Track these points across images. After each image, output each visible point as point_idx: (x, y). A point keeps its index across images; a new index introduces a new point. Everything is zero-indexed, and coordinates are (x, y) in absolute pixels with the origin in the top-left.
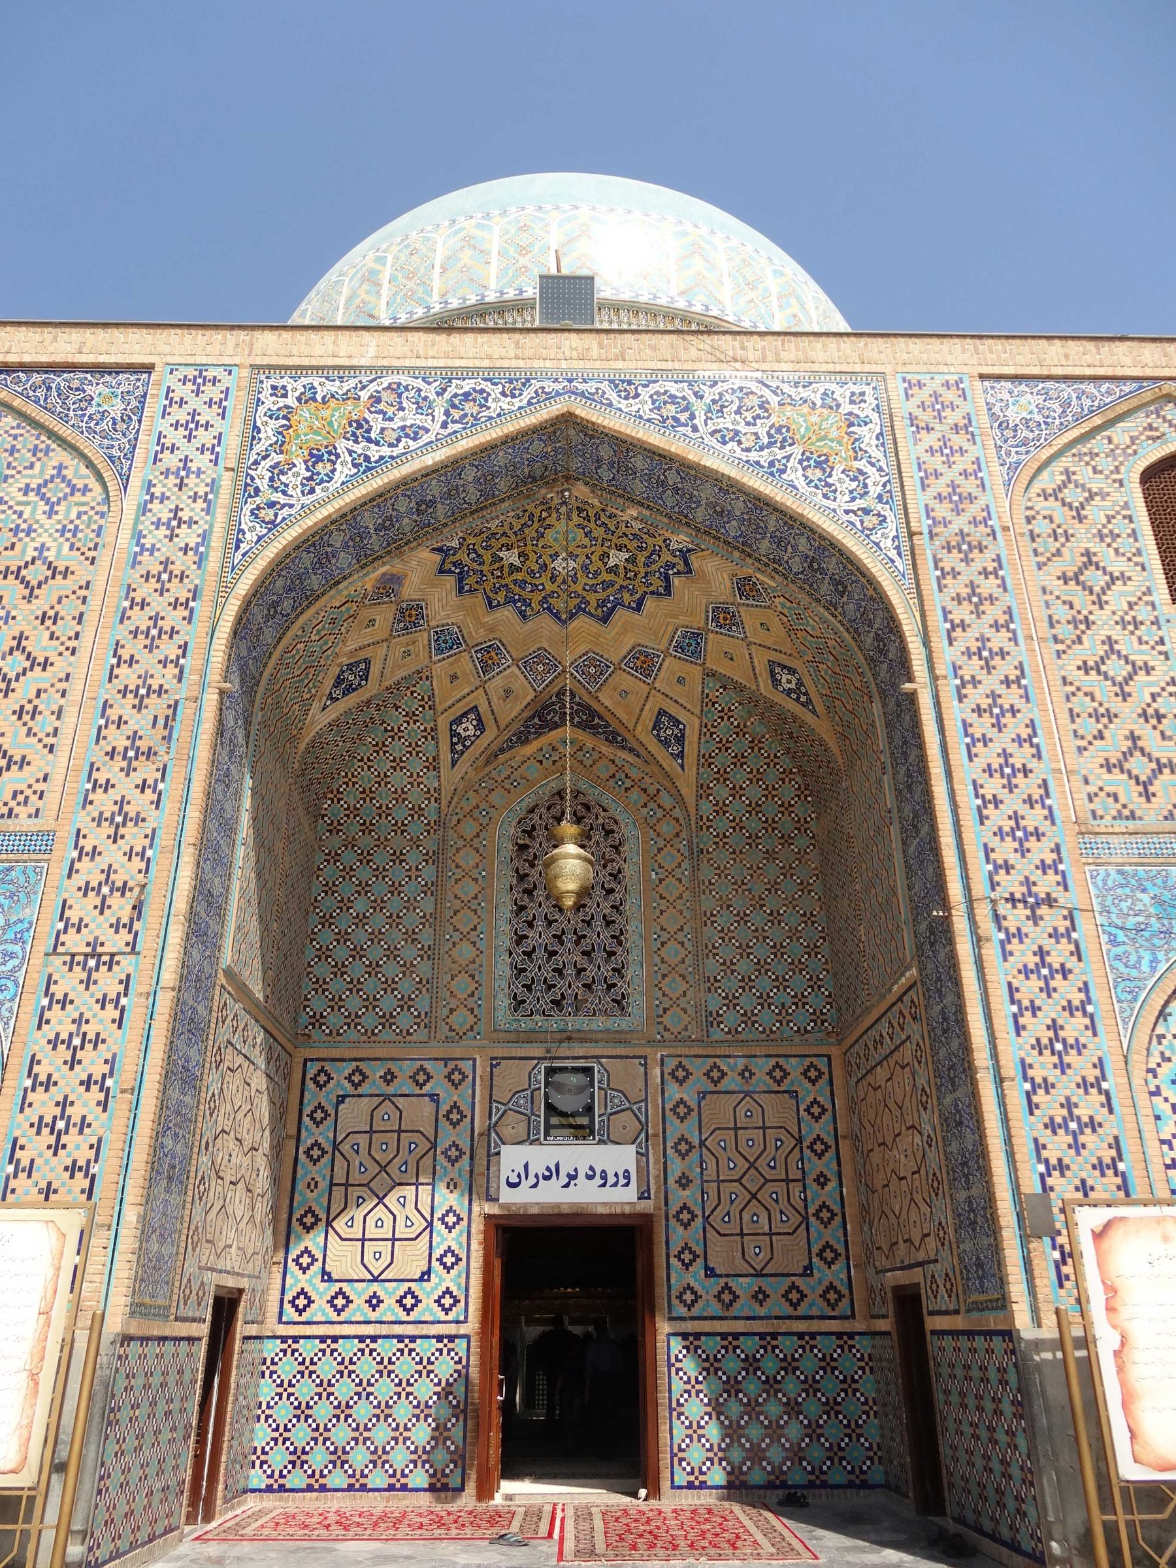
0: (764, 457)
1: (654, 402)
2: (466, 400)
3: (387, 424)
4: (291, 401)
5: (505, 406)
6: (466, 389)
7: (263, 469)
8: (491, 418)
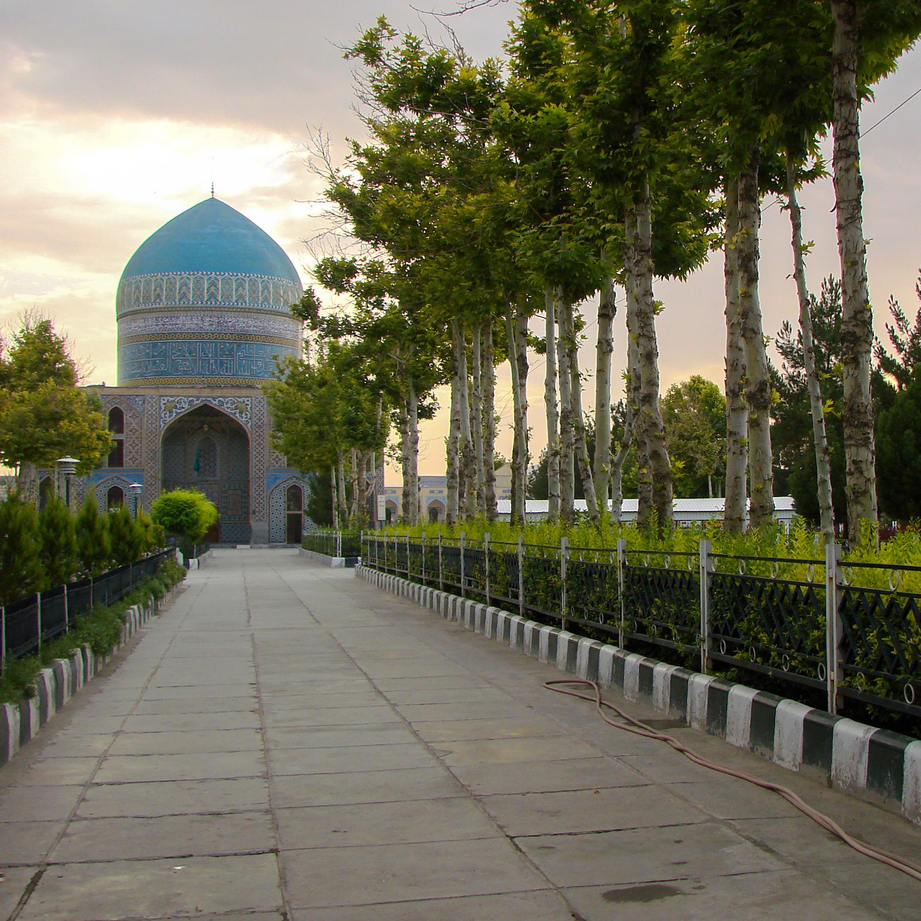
0: (233, 412)
7: (163, 415)
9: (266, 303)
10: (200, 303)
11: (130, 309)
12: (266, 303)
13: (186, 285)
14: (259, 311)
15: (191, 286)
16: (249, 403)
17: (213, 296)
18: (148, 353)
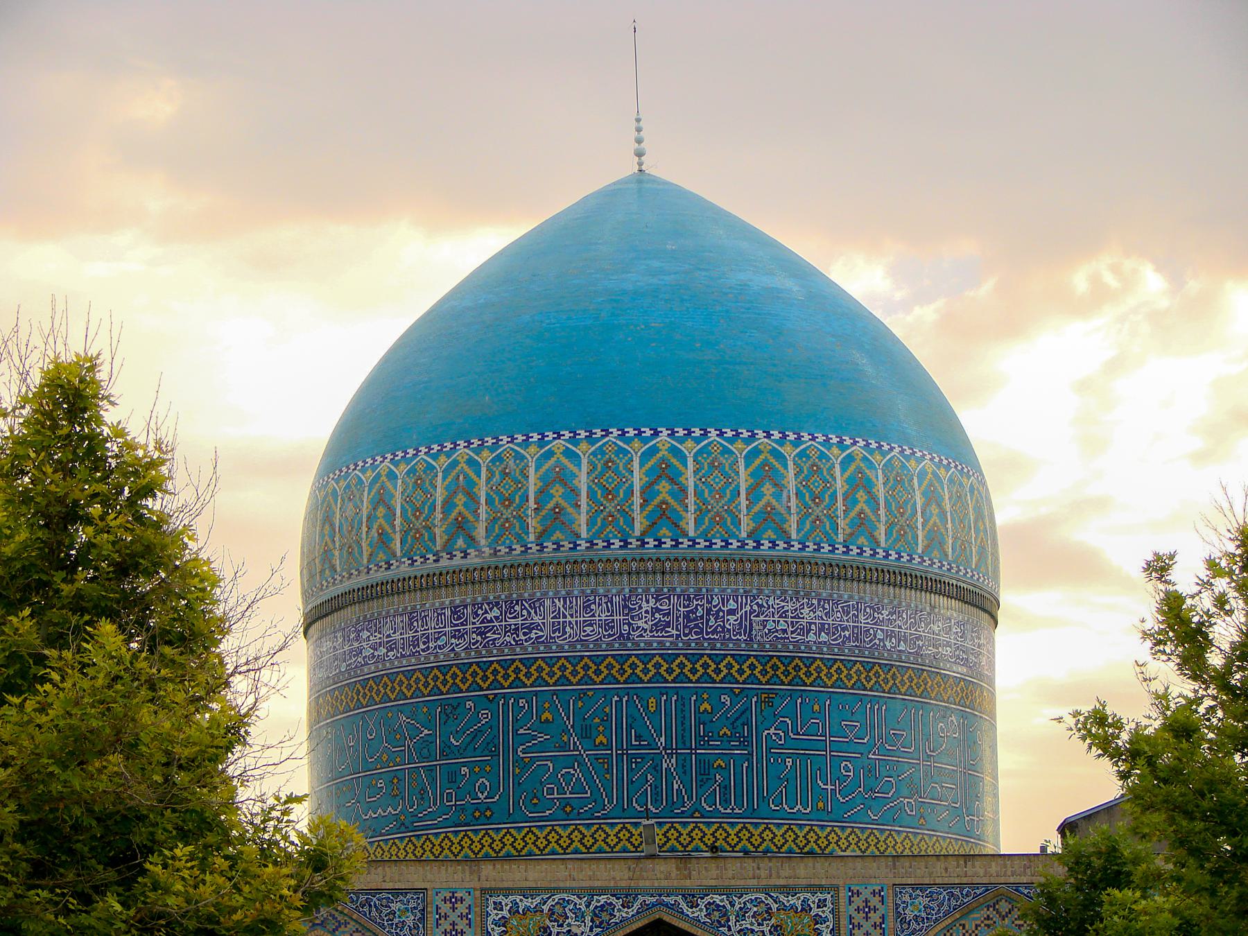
1: (707, 909)
2: (602, 911)
3: (559, 929)
4: (505, 913)
5: (624, 915)
6: (602, 903)
8: (616, 923)
9: (862, 540)
10: (618, 543)
11: (361, 580)
12: (862, 540)
13: (562, 478)
14: (837, 572)
15: (583, 482)
16: (826, 912)
17: (663, 515)
18: (427, 742)
